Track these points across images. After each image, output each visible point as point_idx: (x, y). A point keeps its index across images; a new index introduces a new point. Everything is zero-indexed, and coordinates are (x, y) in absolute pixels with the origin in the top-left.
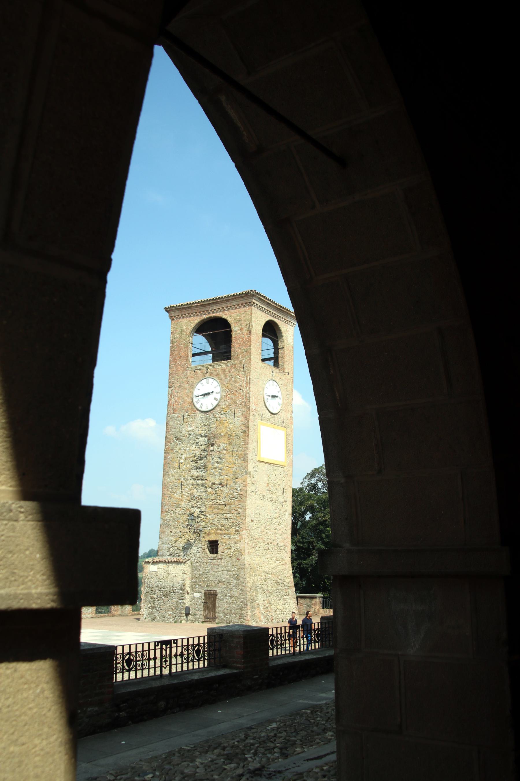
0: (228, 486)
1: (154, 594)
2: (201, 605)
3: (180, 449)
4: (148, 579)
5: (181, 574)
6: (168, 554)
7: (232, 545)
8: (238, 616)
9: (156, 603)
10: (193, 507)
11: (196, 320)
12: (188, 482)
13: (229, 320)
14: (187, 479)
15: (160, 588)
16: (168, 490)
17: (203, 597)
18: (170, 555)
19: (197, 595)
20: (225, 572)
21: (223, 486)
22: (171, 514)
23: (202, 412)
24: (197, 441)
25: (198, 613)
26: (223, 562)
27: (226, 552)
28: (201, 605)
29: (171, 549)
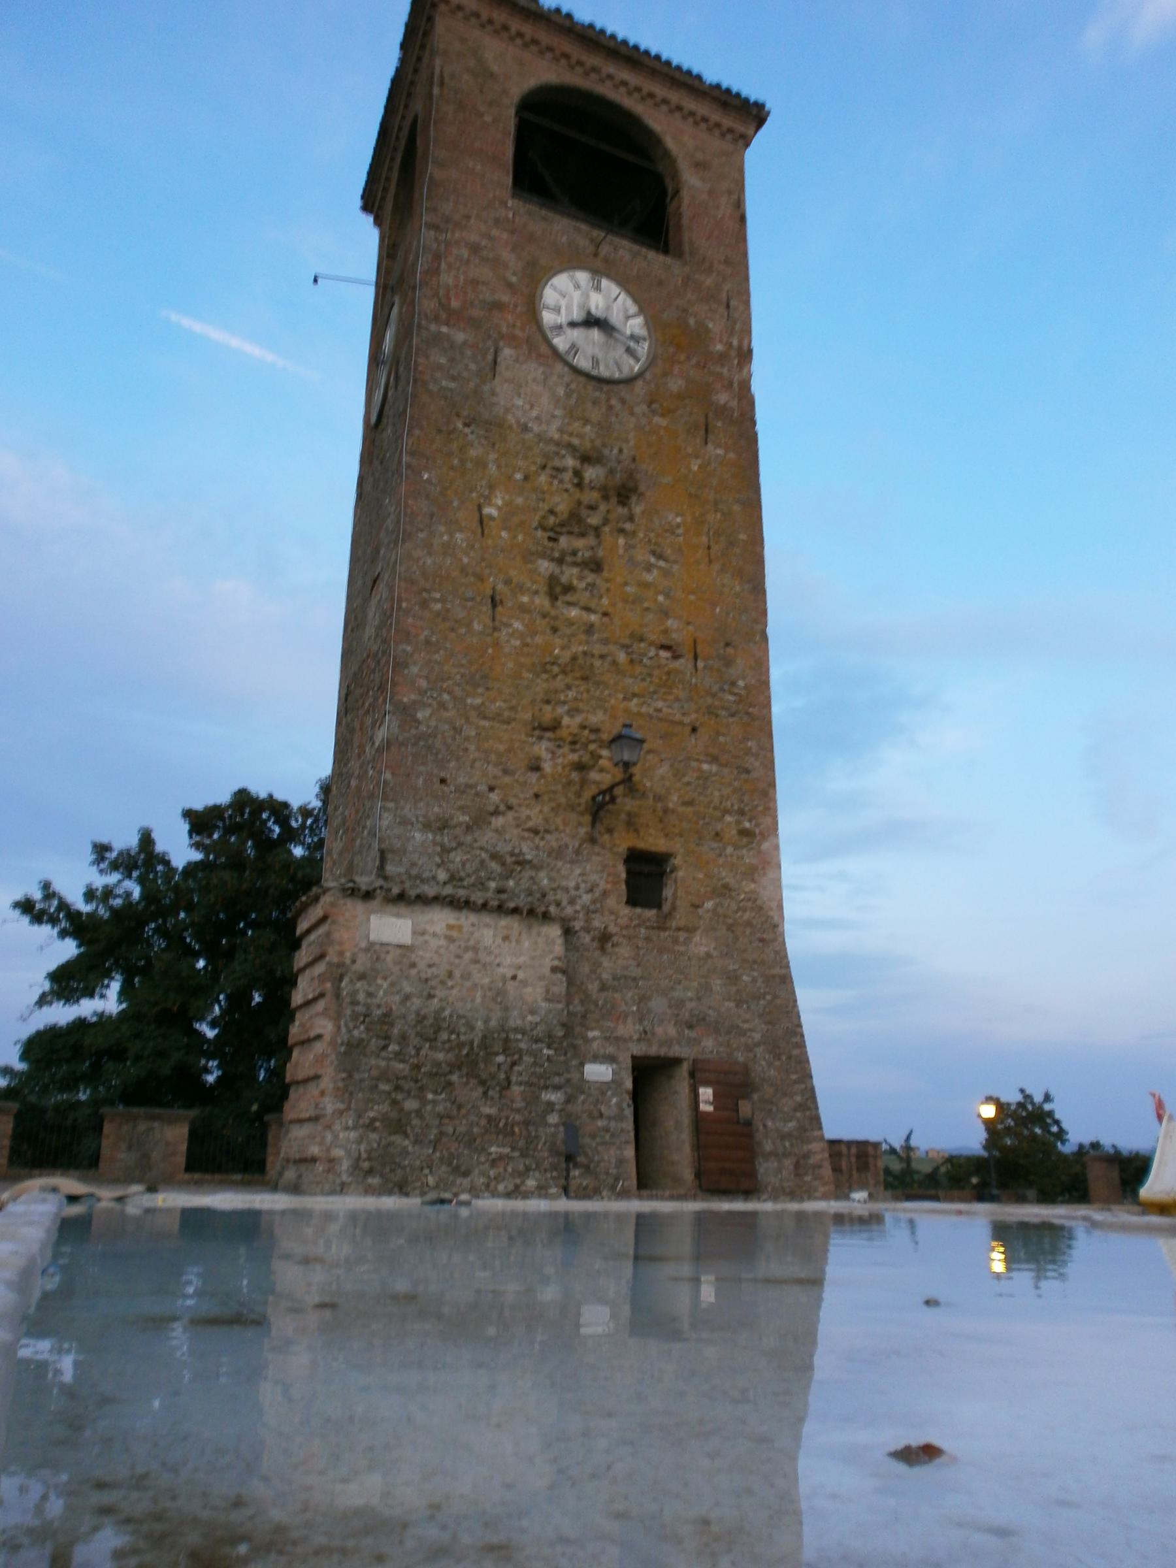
0: (700, 664)
1: (399, 1056)
2: (620, 1117)
3: (481, 464)
4: (362, 977)
5: (546, 971)
6: (442, 876)
7: (730, 880)
8: (788, 1163)
9: (411, 1105)
10: (548, 702)
11: (546, 73)
12: (525, 599)
13: (670, 143)
14: (521, 588)
15: (432, 1029)
16: (424, 604)
17: (629, 1084)
18: (453, 878)
19: (598, 1072)
20: (717, 984)
21: (676, 657)
22: (442, 706)
23: (576, 371)
24: (557, 463)
25: (609, 1156)
26: (701, 945)
27: (709, 905)
28: (620, 1117)
29: (457, 857)
